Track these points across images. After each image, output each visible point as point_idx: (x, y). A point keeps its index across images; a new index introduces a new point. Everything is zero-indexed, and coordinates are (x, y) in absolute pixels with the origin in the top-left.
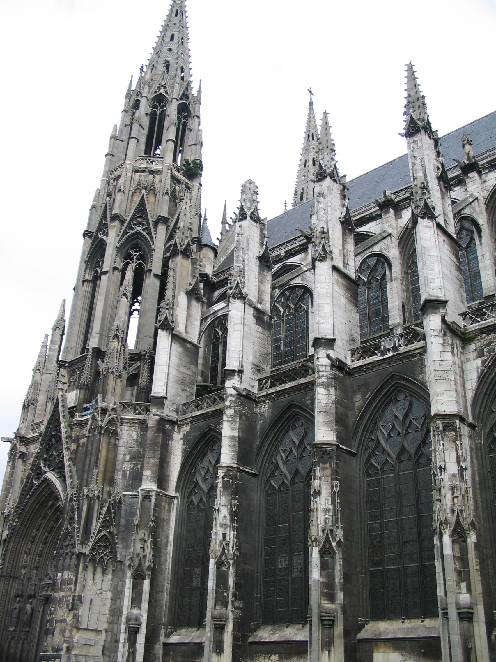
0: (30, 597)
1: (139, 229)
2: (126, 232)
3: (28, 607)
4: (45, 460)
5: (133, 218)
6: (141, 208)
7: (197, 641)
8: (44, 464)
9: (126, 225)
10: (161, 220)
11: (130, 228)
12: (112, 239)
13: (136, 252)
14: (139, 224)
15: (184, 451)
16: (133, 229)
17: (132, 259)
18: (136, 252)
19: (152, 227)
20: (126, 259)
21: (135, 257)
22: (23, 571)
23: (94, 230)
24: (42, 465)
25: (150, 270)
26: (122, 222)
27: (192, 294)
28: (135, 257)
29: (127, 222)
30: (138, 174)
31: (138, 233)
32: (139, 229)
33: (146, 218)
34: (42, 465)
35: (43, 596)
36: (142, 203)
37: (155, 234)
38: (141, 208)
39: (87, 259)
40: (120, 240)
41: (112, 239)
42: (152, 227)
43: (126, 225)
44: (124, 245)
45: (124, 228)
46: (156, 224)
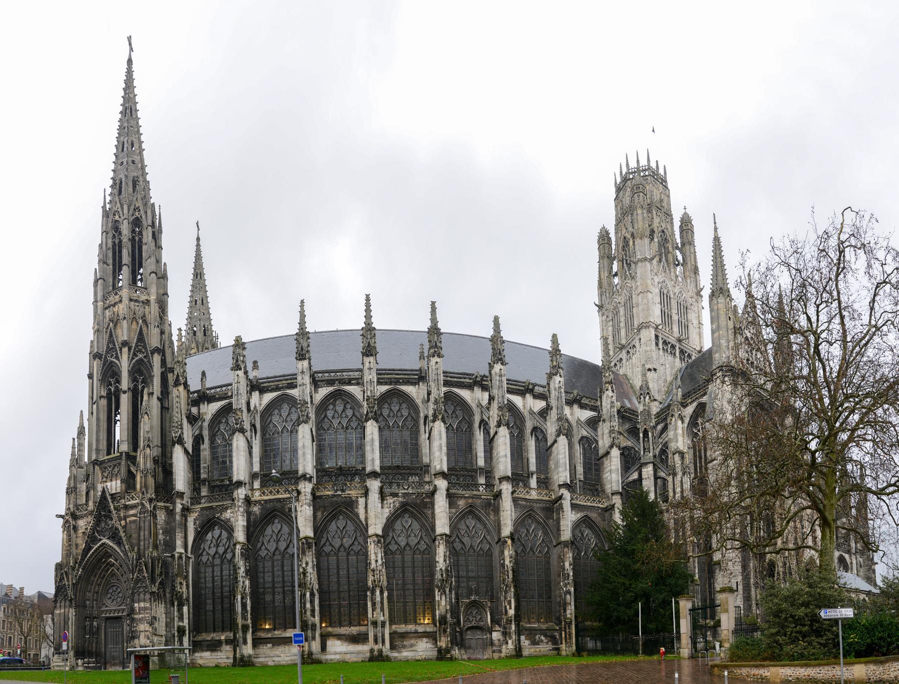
0: (95, 618)
3: (95, 623)
4: (98, 532)
5: (137, 346)
6: (141, 338)
7: (218, 638)
10: (157, 350)
11: (135, 355)
12: (125, 364)
14: (140, 351)
15: (196, 529)
22: (88, 603)
23: (103, 350)
26: (130, 349)
27: (188, 418)
31: (141, 360)
38: (141, 338)
41: (125, 364)
44: (133, 367)
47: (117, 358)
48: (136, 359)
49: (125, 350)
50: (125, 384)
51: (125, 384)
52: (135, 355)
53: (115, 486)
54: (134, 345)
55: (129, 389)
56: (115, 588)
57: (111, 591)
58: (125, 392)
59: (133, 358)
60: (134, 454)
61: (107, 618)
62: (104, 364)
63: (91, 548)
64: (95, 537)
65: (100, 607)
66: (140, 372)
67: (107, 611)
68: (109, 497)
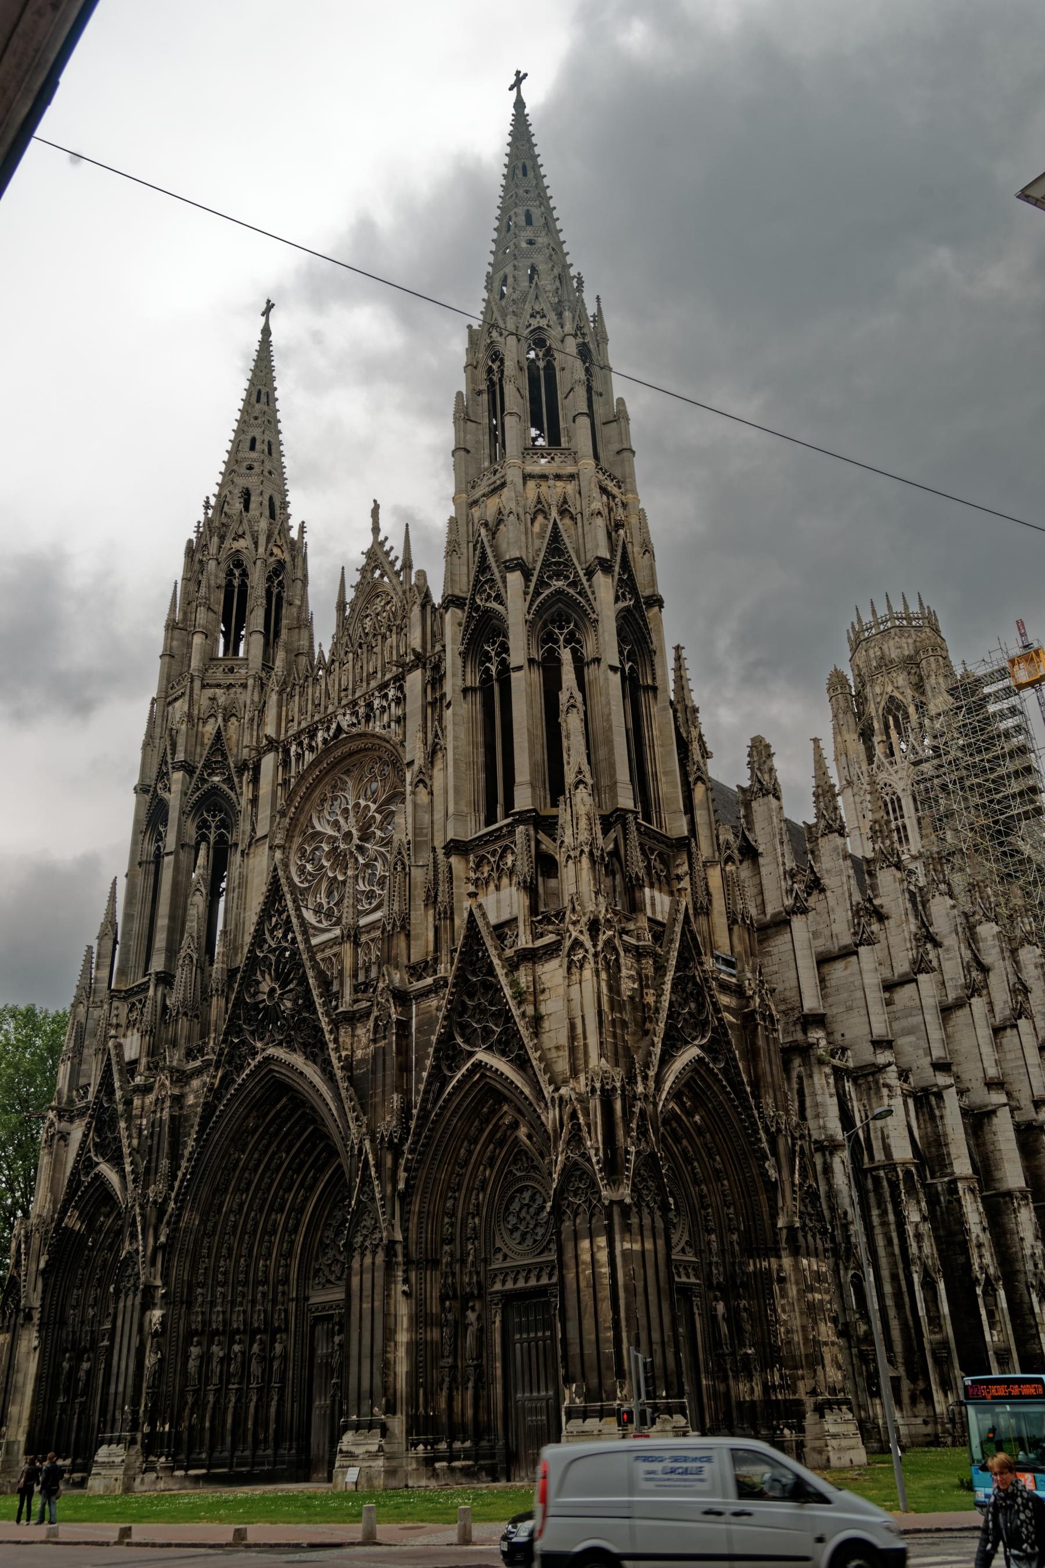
1: (558, 584)
2: (537, 593)
4: (463, 1027)
5: (546, 564)
8: (462, 1036)
9: (534, 579)
11: (542, 584)
12: (515, 607)
13: (561, 628)
14: (558, 575)
16: (549, 585)
17: (556, 641)
18: (561, 628)
19: (584, 579)
20: (545, 642)
21: (562, 638)
24: (459, 1040)
25: (598, 660)
26: (527, 575)
28: (562, 638)
29: (536, 573)
30: (531, 484)
31: (559, 592)
32: (558, 584)
33: (568, 564)
34: (459, 1040)
35: (497, 1292)
36: (556, 536)
37: (593, 593)
39: (462, 648)
40: (530, 608)
41: (515, 607)
42: (584, 579)
43: (534, 579)
44: (538, 613)
45: (532, 585)
46: (590, 574)
47: (499, 599)
48: (547, 592)
49: (515, 579)
50: (519, 647)
51: (519, 647)
52: (542, 584)
53: (504, 902)
54: (538, 569)
55: (531, 661)
56: (527, 1195)
57: (516, 1206)
58: (519, 668)
59: (537, 593)
60: (553, 811)
61: (509, 1299)
62: (470, 617)
63: (445, 1081)
64: (455, 1046)
65: (487, 1261)
66: (560, 618)
67: (505, 1273)
68: (484, 932)
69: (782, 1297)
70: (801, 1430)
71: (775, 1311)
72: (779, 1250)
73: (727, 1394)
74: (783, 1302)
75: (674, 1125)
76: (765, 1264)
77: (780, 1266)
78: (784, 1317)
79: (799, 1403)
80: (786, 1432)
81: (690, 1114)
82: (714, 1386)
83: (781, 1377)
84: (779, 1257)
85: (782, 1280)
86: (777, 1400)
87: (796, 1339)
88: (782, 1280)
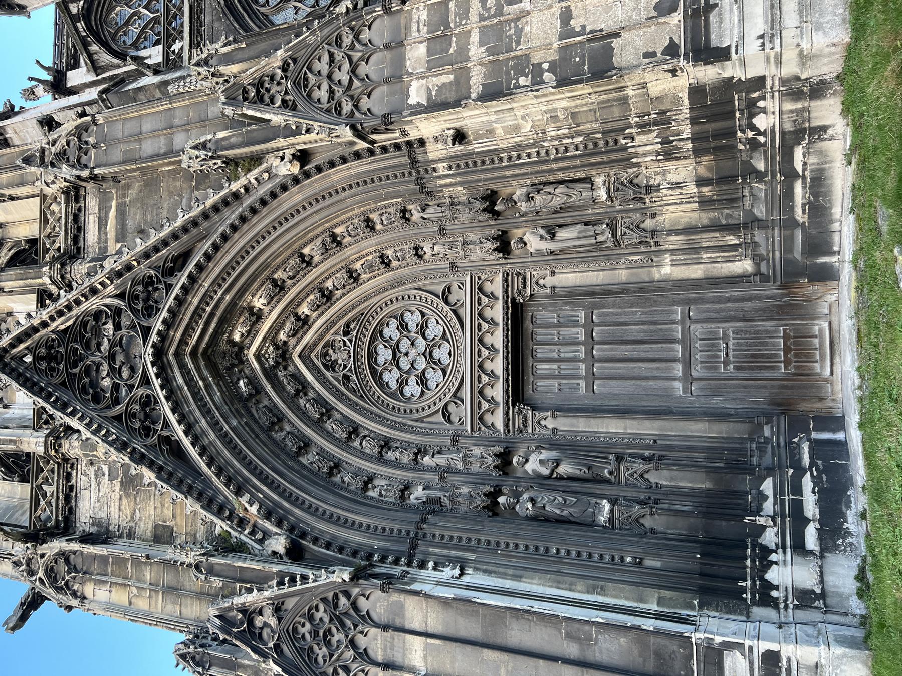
69: (491, 132)
70: (760, 82)
71: (519, 147)
72: (409, 144)
73: (689, 230)
74: (500, 132)
75: (282, 336)
76: (442, 168)
77: (436, 139)
78: (527, 127)
79: (696, 91)
80: (761, 122)
81: (257, 317)
82: (673, 252)
83: (644, 127)
84: (422, 142)
85: (460, 137)
86: (693, 139)
87: (564, 103)
88: (460, 137)
